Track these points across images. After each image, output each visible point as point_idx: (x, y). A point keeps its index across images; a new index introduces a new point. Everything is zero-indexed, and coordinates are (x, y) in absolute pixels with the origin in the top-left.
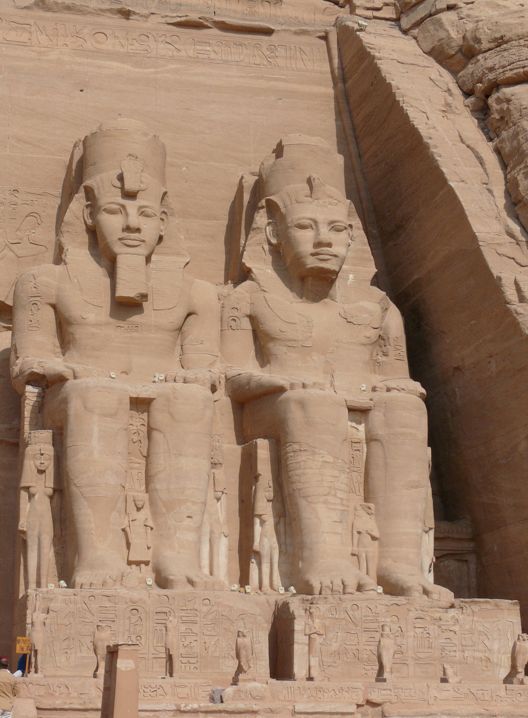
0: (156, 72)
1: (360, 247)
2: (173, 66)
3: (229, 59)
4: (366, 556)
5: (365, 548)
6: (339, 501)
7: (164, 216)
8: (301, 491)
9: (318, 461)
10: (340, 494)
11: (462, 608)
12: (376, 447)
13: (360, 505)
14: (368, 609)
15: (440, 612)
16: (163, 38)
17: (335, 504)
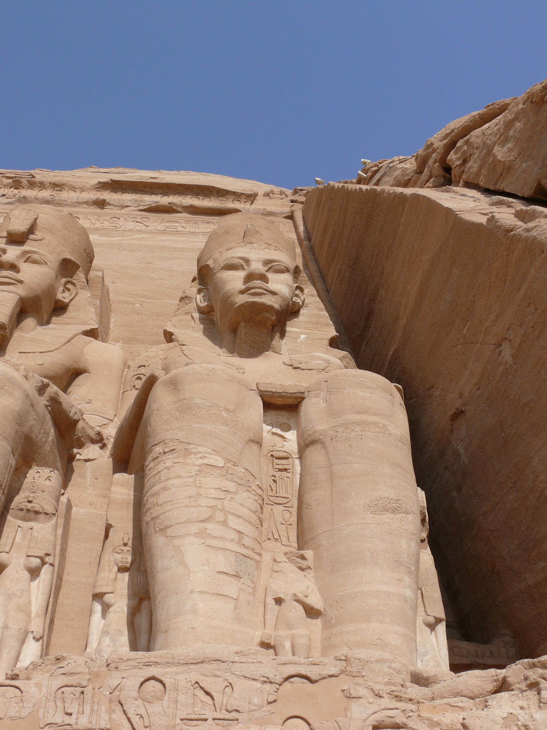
0: (122, 240)
1: (315, 312)
2: (140, 236)
3: (197, 231)
4: (293, 646)
5: (291, 628)
6: (234, 535)
7: (69, 286)
8: (158, 522)
9: (194, 465)
10: (233, 522)
11: (534, 686)
12: (315, 455)
13: (285, 554)
14: (200, 693)
15: (463, 709)
16: (134, 219)
17: (222, 538)
